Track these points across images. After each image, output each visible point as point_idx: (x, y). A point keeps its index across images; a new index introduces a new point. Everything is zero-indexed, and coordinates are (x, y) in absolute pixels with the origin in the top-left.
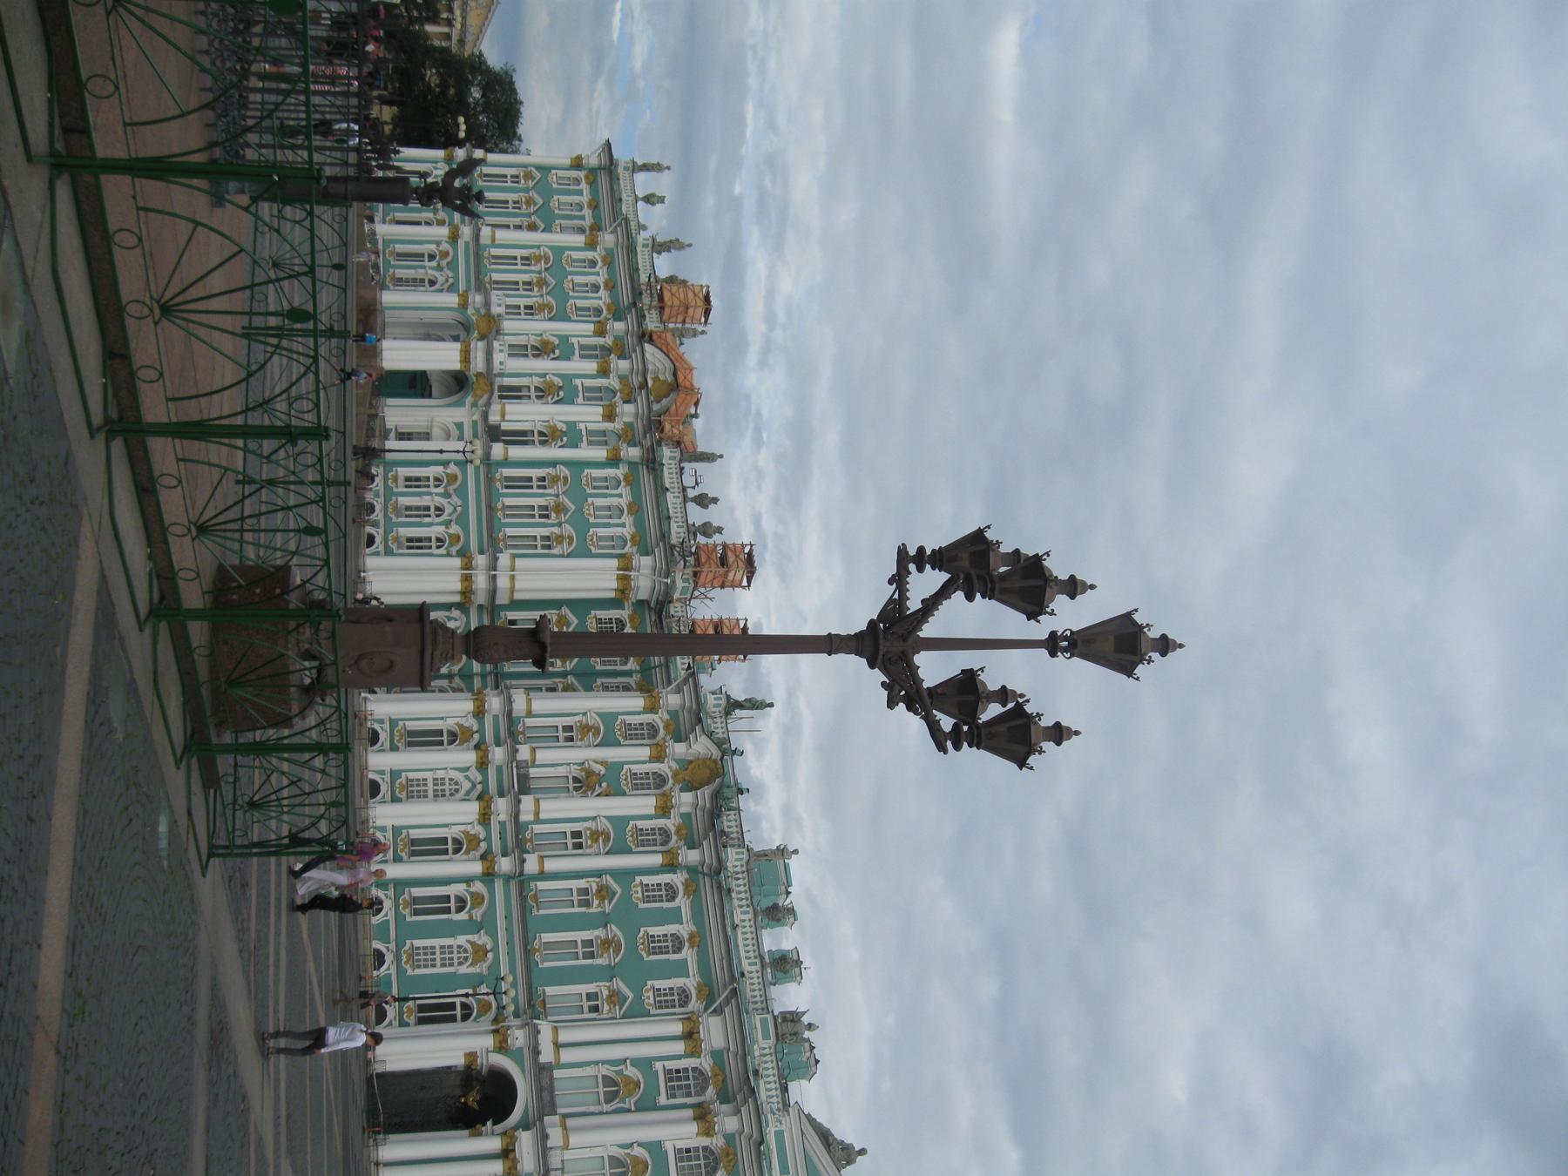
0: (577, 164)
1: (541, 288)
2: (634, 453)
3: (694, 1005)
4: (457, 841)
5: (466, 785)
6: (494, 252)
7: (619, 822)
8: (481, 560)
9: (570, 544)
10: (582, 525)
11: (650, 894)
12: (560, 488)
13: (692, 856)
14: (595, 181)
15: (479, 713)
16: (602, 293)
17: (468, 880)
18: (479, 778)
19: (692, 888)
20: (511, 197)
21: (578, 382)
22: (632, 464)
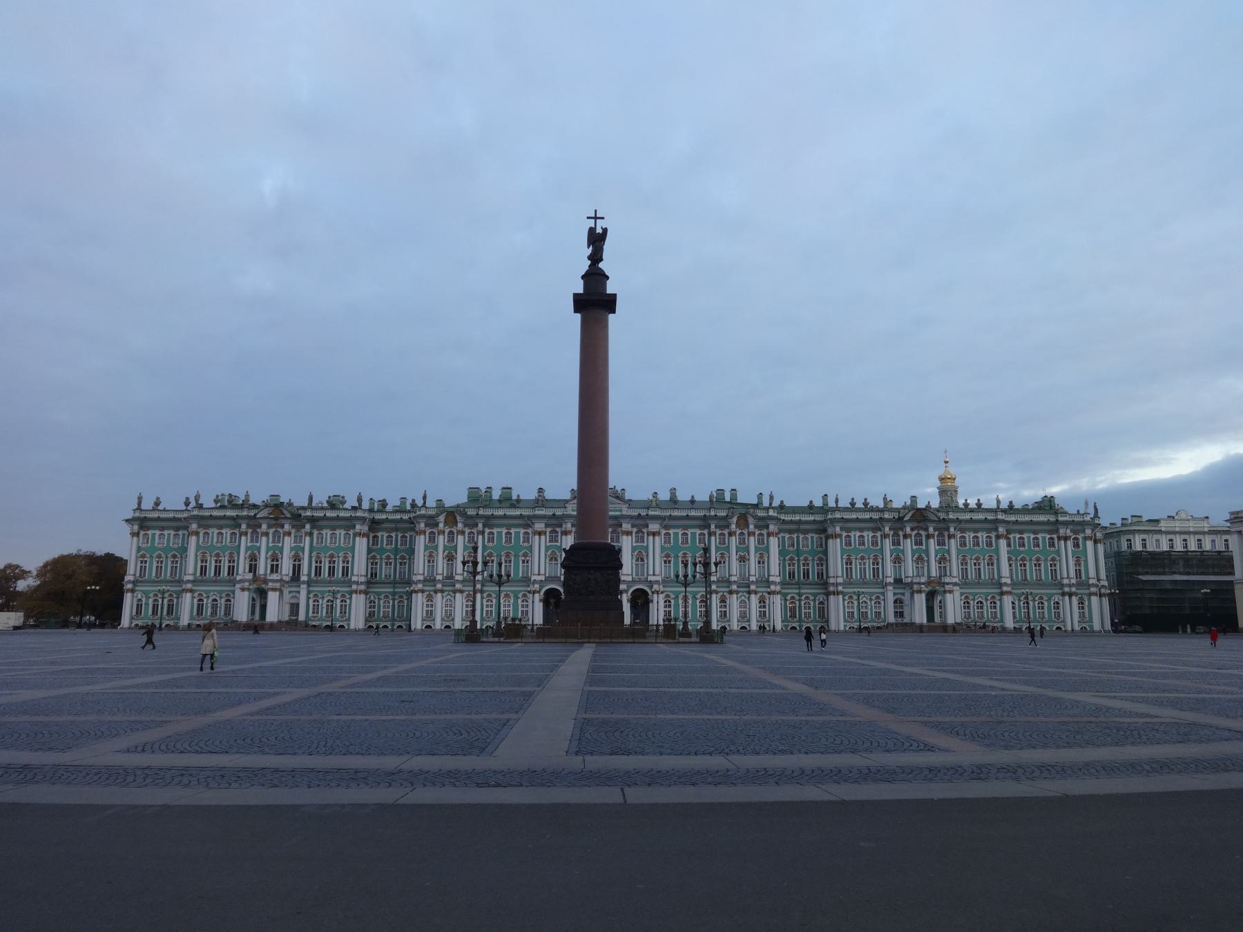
0: (133, 534)
2: (308, 527)
3: (530, 531)
8: (354, 587)
10: (339, 549)
11: (491, 540)
12: (322, 555)
13: (480, 526)
15: (423, 591)
17: (482, 598)
19: (491, 527)
20: (155, 564)
22: (312, 528)
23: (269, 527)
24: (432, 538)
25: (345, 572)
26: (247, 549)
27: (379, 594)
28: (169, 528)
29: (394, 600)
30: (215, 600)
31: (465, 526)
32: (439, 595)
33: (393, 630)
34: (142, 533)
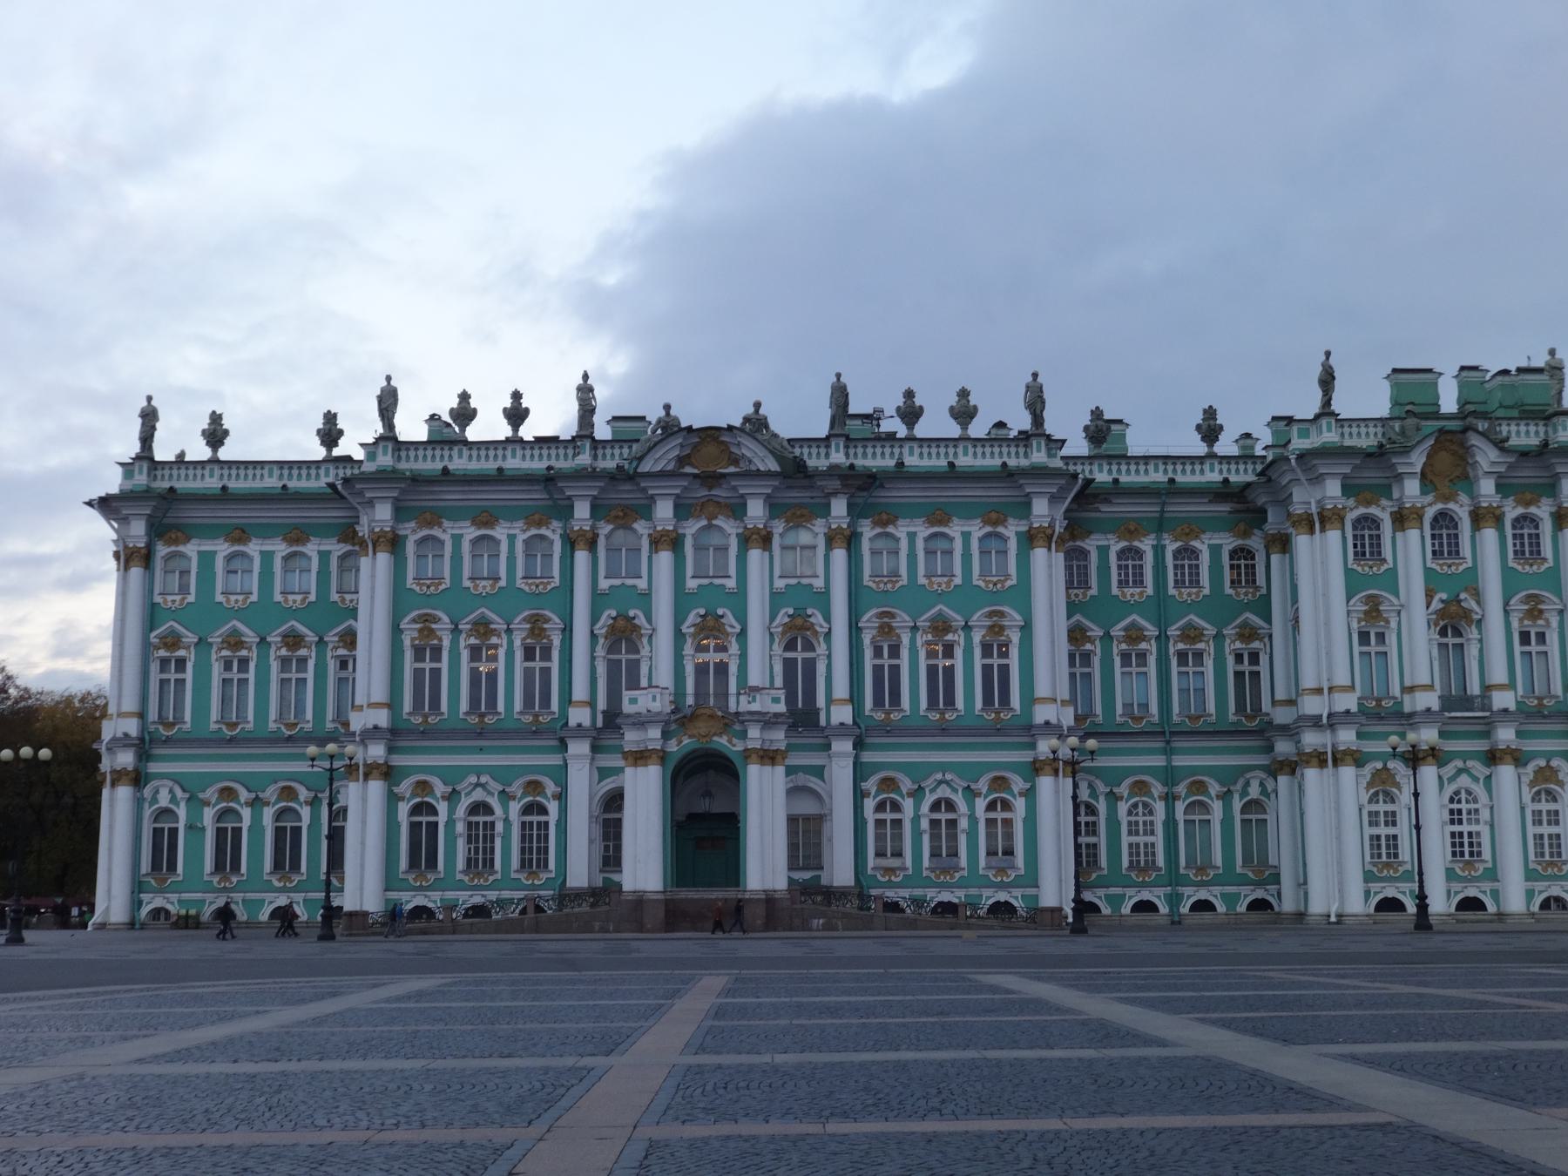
0: (127, 557)
1: (494, 632)
2: (839, 507)
4: (1536, 798)
5: (1464, 781)
6: (407, 706)
7: (1510, 582)
8: (1044, 747)
9: (1002, 614)
10: (966, 595)
12: (903, 619)
14: (178, 528)
15: (1359, 759)
16: (500, 532)
18: (1459, 763)
21: (692, 584)
23: (683, 510)
24: (1366, 545)
25: (996, 685)
26: (598, 600)
27: (1113, 777)
28: (266, 531)
29: (1170, 799)
30: (480, 808)
31: (1501, 488)
32: (1428, 773)
33: (1176, 922)
34: (162, 550)
